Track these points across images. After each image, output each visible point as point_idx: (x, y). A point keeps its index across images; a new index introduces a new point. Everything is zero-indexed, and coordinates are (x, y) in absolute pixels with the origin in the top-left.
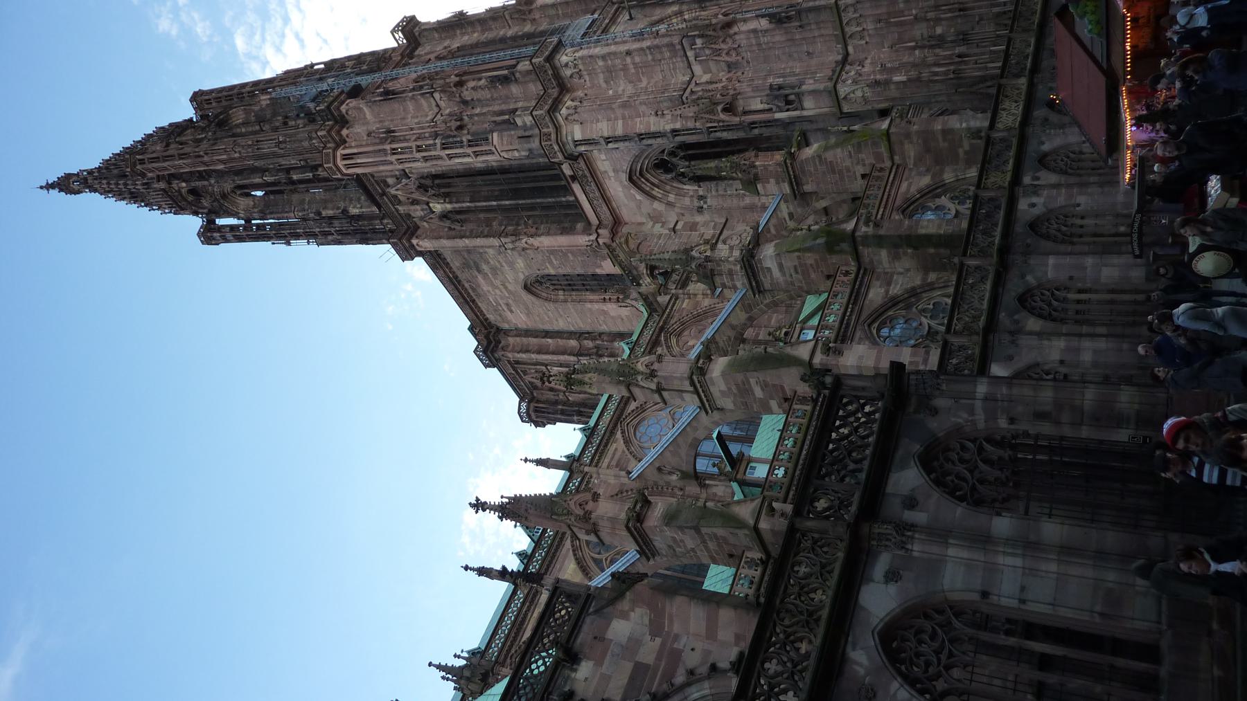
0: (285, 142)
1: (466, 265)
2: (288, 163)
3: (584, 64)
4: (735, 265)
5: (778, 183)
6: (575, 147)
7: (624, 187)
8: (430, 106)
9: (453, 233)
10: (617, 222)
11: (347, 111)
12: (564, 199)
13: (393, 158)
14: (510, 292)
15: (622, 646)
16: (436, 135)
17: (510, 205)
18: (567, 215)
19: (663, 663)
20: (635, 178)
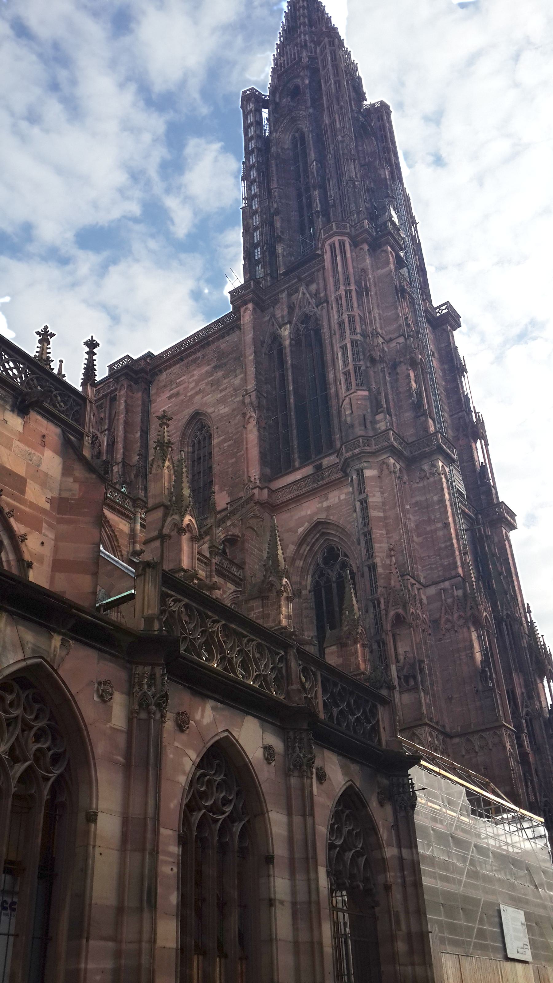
0: (355, 187)
2: (331, 188)
3: (435, 482)
4: (274, 621)
6: (356, 470)
7: (312, 516)
11: (386, 252)
12: (296, 456)
14: (192, 397)
15: (39, 466)
16: (364, 335)
17: (290, 403)
19: (27, 509)
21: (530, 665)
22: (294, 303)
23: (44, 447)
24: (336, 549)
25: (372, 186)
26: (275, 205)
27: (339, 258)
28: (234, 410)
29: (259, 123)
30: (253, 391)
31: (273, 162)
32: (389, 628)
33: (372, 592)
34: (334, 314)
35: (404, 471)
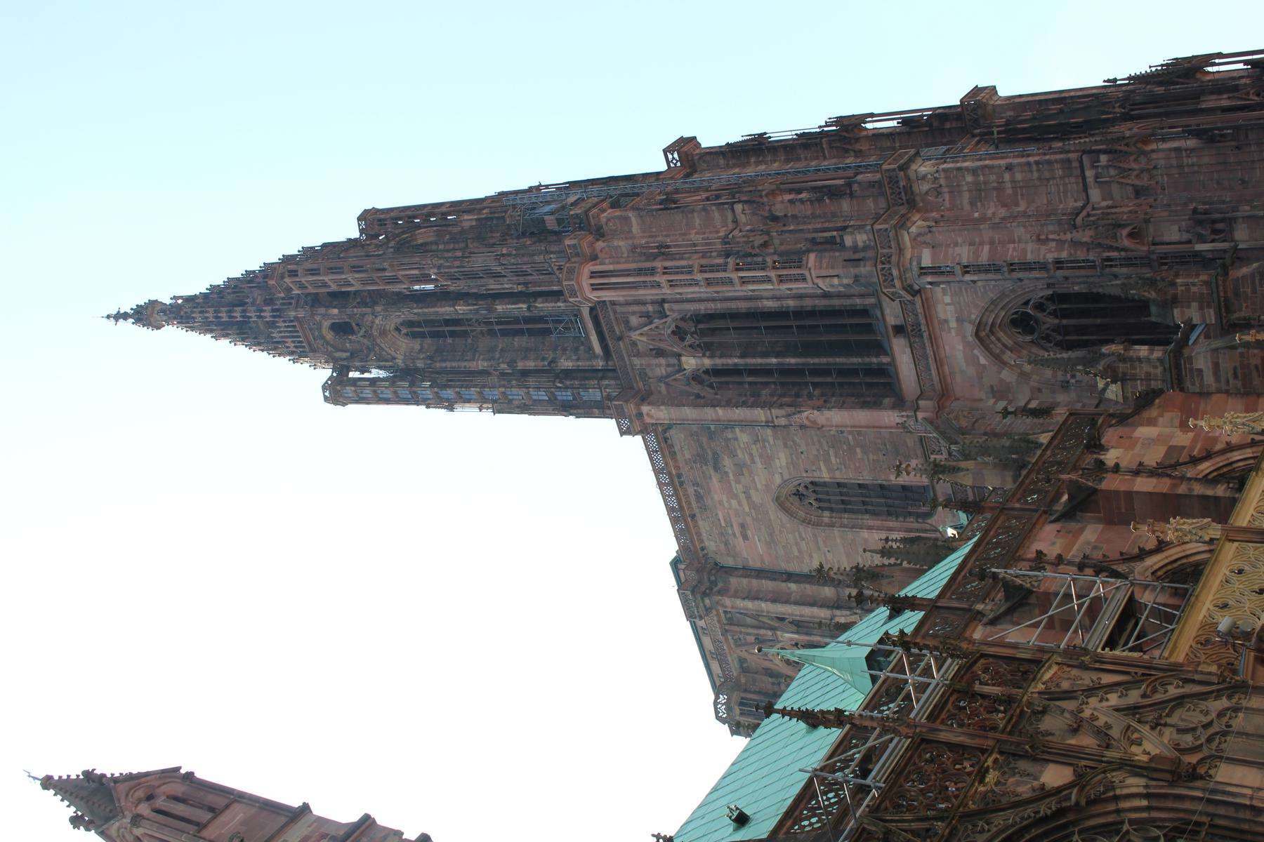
0: (509, 255)
1: (700, 458)
2: (499, 287)
3: (947, 178)
4: (1155, 367)
5: (1201, 308)
6: (919, 276)
8: (725, 224)
9: (702, 401)
10: (944, 394)
11: (608, 220)
12: (874, 360)
13: (662, 279)
16: (728, 255)
17: (796, 364)
18: (870, 385)
20: (983, 334)
21: (1189, 85)
22: (651, 350)
23: (1131, 438)
24: (1014, 316)
25: (498, 235)
26: (503, 366)
27: (613, 280)
28: (786, 446)
29: (373, 381)
30: (771, 413)
31: (438, 365)
32: (1145, 248)
33: (1094, 267)
34: (690, 292)
35: (927, 215)
